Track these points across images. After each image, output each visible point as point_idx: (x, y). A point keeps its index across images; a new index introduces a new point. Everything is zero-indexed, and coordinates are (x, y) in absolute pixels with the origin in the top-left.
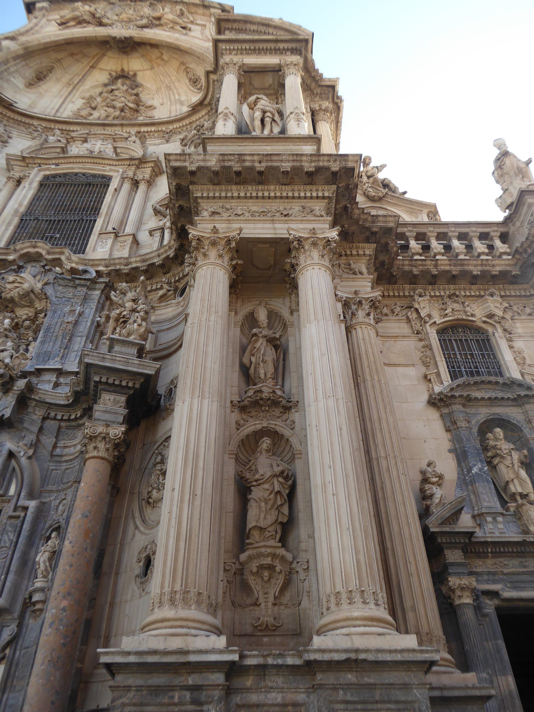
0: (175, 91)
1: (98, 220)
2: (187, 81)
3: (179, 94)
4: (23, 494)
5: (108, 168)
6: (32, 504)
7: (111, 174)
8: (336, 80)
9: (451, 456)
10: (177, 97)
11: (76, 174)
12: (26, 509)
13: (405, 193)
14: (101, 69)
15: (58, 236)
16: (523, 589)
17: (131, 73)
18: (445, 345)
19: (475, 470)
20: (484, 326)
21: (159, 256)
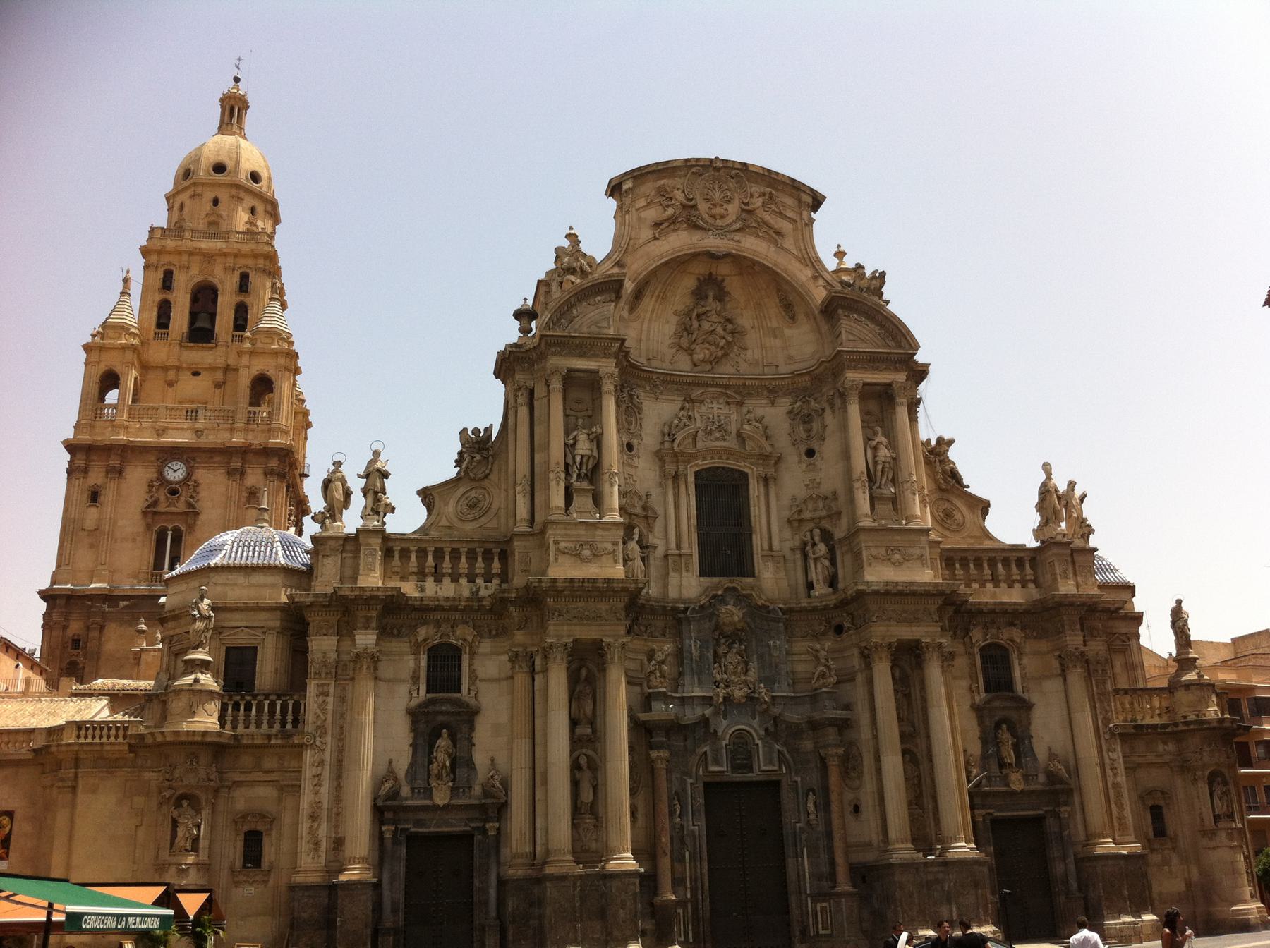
0: (766, 316)
1: (754, 536)
2: (777, 301)
3: (770, 321)
4: (793, 774)
5: (743, 464)
6: (799, 779)
7: (745, 470)
8: (927, 366)
9: (979, 741)
10: (769, 325)
11: (718, 467)
12: (796, 782)
13: (968, 487)
14: (690, 273)
15: (729, 552)
16: (1002, 811)
17: (719, 278)
18: (984, 660)
19: (990, 751)
20: (1007, 646)
21: (821, 602)
